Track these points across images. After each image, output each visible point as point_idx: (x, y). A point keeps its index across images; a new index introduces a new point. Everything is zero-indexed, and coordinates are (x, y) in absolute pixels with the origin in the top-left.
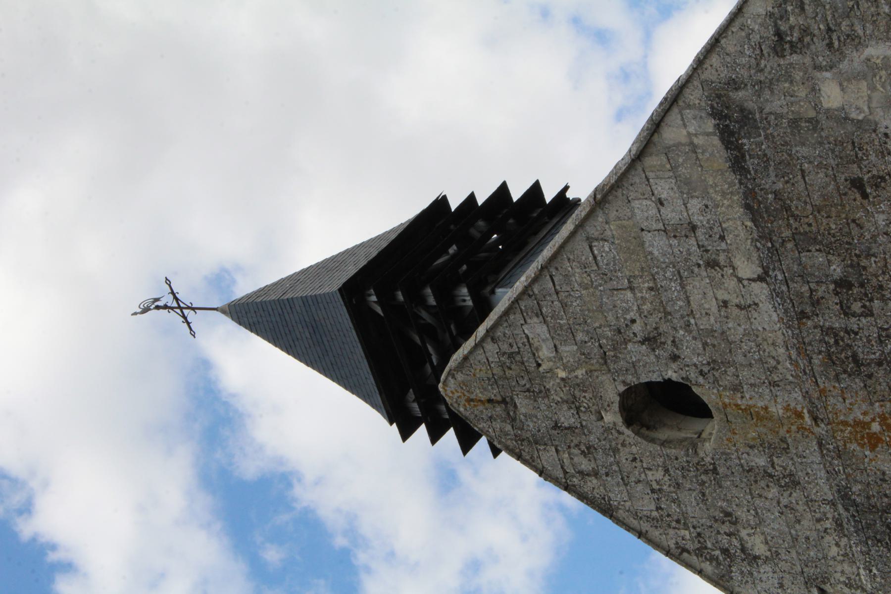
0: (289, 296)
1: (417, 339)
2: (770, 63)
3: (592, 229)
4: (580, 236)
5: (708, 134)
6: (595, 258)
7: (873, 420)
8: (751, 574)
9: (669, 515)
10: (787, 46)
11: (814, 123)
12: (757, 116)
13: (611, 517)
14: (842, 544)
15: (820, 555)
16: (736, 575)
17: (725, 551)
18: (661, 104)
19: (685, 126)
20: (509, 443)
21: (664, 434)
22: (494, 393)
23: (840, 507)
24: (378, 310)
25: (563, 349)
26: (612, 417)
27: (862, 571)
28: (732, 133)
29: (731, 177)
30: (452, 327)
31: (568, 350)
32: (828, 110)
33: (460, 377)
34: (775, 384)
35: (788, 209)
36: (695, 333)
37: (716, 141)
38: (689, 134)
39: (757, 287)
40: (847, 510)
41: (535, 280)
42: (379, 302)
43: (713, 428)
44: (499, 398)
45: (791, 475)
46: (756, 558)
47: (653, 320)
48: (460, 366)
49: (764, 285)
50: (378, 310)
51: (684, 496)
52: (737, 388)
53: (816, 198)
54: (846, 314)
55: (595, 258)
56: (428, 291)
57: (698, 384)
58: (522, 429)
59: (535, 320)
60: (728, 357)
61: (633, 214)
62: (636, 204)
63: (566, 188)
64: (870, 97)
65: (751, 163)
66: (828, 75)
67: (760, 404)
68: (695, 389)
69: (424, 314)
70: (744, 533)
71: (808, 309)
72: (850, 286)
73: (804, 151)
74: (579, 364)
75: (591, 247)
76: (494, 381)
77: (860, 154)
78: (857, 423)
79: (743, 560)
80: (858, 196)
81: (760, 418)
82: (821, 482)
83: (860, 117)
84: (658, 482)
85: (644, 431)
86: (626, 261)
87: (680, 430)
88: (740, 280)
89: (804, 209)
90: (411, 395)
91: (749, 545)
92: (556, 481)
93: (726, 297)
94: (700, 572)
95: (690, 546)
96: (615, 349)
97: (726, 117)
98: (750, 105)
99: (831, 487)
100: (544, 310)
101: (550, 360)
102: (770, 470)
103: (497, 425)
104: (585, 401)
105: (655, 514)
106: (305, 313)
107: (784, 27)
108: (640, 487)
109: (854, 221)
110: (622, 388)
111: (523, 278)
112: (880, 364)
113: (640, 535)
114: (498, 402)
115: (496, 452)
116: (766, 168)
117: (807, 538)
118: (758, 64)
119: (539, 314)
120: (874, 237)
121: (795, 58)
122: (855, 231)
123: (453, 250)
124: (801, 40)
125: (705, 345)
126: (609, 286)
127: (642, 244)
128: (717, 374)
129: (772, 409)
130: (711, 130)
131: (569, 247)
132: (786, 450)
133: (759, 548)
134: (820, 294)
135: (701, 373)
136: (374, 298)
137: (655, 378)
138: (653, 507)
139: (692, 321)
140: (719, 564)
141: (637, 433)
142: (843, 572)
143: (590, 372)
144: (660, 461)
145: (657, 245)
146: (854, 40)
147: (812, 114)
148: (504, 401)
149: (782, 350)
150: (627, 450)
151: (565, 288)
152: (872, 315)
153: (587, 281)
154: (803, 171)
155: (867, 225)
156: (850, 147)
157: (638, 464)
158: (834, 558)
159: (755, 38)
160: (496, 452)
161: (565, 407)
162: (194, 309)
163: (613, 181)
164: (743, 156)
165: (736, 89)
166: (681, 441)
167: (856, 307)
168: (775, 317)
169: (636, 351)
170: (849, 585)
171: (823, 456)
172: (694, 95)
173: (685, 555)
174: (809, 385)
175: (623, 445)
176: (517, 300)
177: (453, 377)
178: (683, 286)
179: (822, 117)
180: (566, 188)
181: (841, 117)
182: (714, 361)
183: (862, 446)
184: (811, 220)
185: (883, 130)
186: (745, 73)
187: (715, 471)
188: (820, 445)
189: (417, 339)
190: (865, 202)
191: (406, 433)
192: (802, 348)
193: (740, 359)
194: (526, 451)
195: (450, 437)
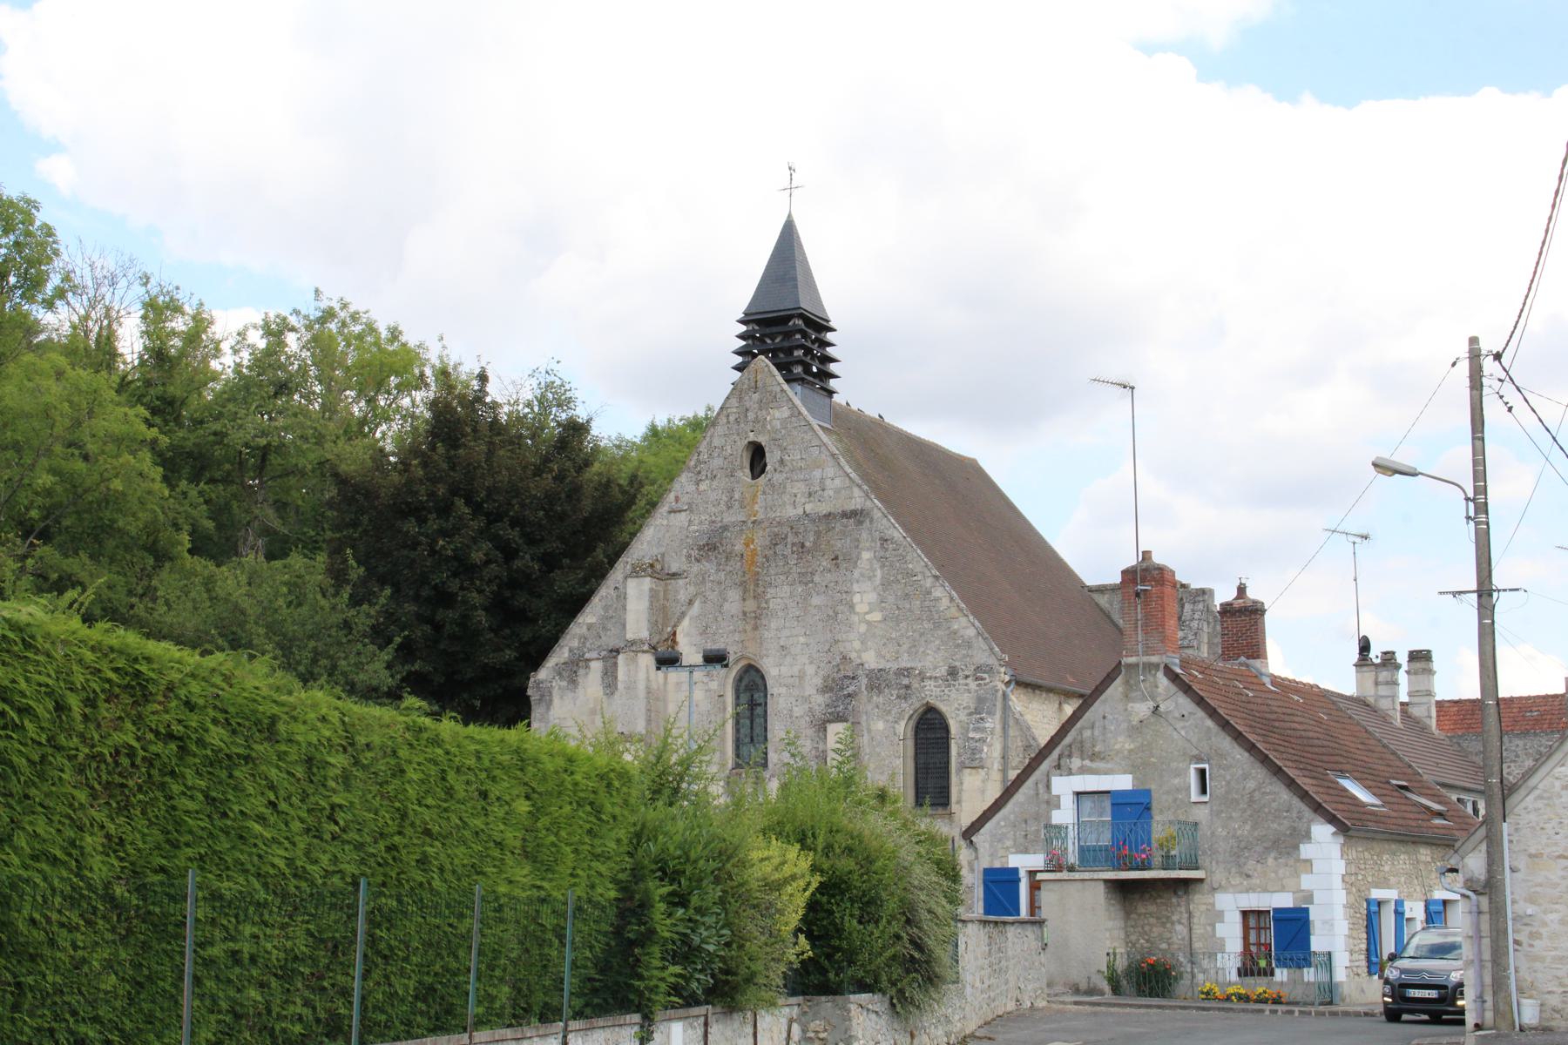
11: (857, 547)
17: (699, 472)
22: (760, 384)
26: (752, 437)
52: (764, 493)
76: (765, 385)
119: (792, 415)
133: (703, 487)
145: (817, 474)
146: (883, 566)
181: (858, 557)
195: (739, 359)
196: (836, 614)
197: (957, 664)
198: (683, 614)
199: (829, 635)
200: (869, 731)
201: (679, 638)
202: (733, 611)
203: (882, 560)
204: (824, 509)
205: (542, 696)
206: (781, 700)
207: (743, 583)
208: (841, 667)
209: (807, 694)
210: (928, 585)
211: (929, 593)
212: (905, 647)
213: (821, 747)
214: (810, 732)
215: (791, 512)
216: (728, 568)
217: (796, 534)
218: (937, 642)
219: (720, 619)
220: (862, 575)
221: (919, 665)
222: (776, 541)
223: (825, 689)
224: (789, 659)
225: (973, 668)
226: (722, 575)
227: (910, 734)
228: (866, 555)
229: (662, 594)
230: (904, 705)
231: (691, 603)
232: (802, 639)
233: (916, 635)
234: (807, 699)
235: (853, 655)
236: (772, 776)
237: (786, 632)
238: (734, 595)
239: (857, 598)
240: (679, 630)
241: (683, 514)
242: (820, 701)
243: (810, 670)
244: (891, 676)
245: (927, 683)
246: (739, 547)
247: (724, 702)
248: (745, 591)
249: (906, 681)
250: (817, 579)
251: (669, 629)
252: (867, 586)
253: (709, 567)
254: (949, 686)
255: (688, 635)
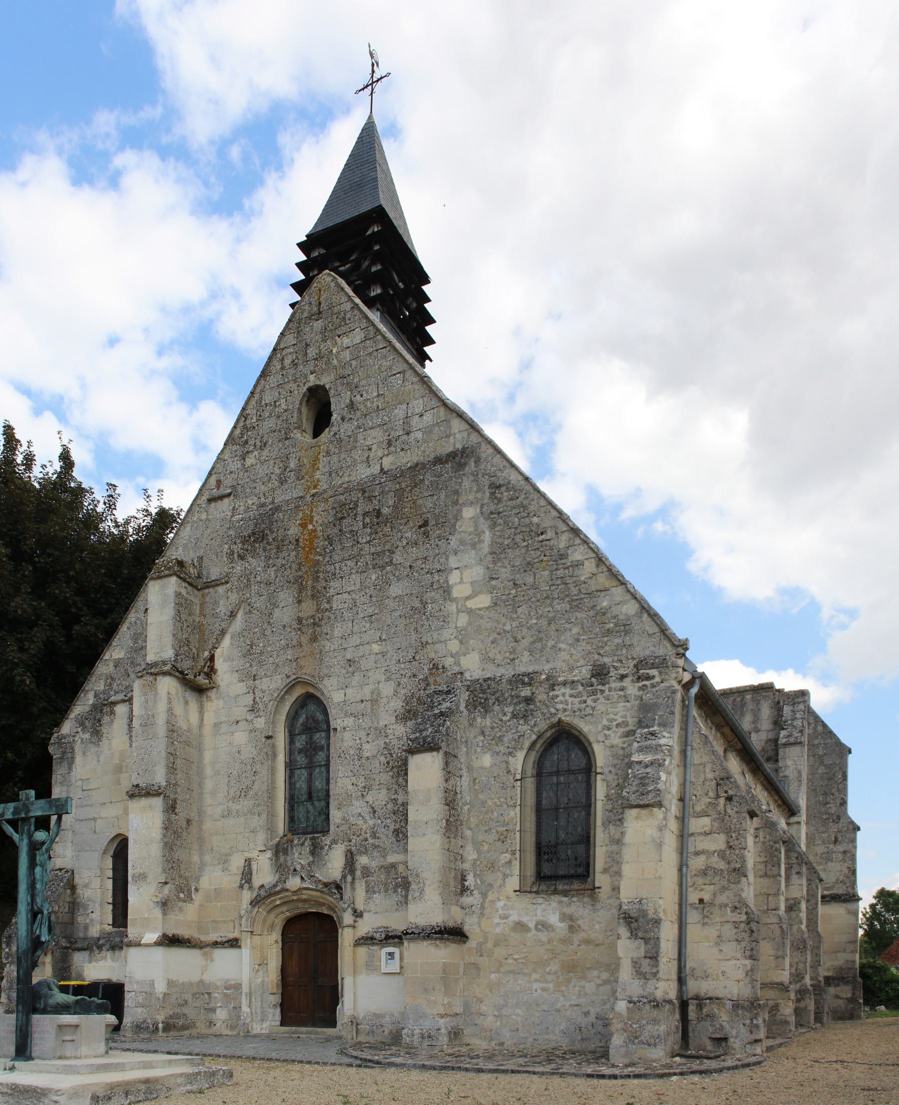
0: (378, 168)
1: (353, 258)
2: (486, 481)
3: (409, 373)
4: (406, 366)
5: (454, 445)
6: (395, 375)
7: (314, 526)
8: (236, 456)
9: (263, 411)
10: (493, 490)
11: (456, 503)
12: (461, 473)
13: (261, 376)
14: (253, 506)
15: (247, 494)
16: (235, 448)
17: (246, 442)
18: (471, 419)
19: (459, 432)
20: (298, 314)
21: (304, 410)
22: (324, 307)
23: (271, 506)
24: (369, 232)
25: (348, 351)
26: (312, 380)
27: (241, 516)
28: (454, 458)
29: (432, 456)
30: (359, 282)
31: (346, 355)
32: (461, 510)
33: (333, 285)
34: (330, 475)
35: (415, 486)
36: (355, 431)
37: (451, 449)
38: (455, 434)
39: (378, 467)
40: (270, 510)
41: (384, 337)
42: (373, 233)
43: (308, 439)
44: (321, 310)
45: (286, 481)
46: (244, 459)
47: (362, 407)
48: (338, 285)
49: (379, 472)
50: (369, 232)
51: (273, 420)
52: (328, 454)
53: (420, 502)
54: (364, 514)
55: (395, 375)
56: (379, 267)
57: (330, 431)
58: (305, 323)
59: (363, 336)
60: (343, 449)
61: (416, 399)
62: (421, 401)
63: (431, 360)
64: (466, 532)
65: (438, 467)
66: (478, 511)
67: (320, 466)
68: (327, 430)
69: (366, 263)
70: (256, 453)
71: (366, 495)
72: (378, 517)
73: (443, 497)
74: (340, 362)
75: (400, 373)
77: (440, 526)
78: (312, 517)
79: (242, 452)
80: (420, 523)
81: (314, 465)
82: (283, 497)
83: (457, 527)
84: (279, 405)
85: (306, 399)
86: (392, 393)
87: (307, 420)
88: (381, 458)
89: (415, 495)
90: (322, 251)
91: (250, 456)
92: (278, 343)
93: (373, 450)
94: (235, 427)
95: (248, 422)
96: (347, 384)
97: (462, 455)
98: (467, 469)
99: (281, 502)
100: (368, 342)
101: (342, 343)
102: (288, 470)
103: (307, 308)
104: (322, 364)
105: (263, 402)
106: (369, 179)
107: (503, 489)
108: (277, 394)
109: (408, 521)
110: (327, 387)
111: (385, 329)
112: (340, 531)
113: (252, 393)
114: (319, 309)
115: (292, 306)
116: (435, 476)
117: (255, 488)
118: (486, 474)
119: (366, 339)
120: (400, 531)
121: (488, 494)
122: (403, 521)
123: (401, 285)
124: (496, 498)
125: (349, 437)
126: (380, 382)
127: (400, 403)
128: (335, 442)
129: (318, 472)
130: (456, 447)
131: (400, 359)
132: (298, 479)
133: (250, 461)
134: (374, 501)
135: (336, 434)
136: (376, 229)
137: (333, 407)
138: (267, 402)
139: (361, 430)
140: (240, 438)
141: (304, 394)
142: (240, 506)
143: (335, 368)
144: (291, 407)
145: (400, 412)
146: (494, 525)
147: (460, 502)
148: (320, 313)
149: (347, 479)
150: (296, 388)
151: (379, 355)
152: (364, 528)
153: (383, 369)
154: (433, 495)
155: (406, 528)
156: (443, 521)
157: (289, 394)
158: (246, 502)
159: (499, 474)
160: (292, 306)
161: (317, 351)
162: (372, 94)
163: (433, 388)
164: (442, 464)
165: (475, 462)
166: (300, 420)
167: (367, 520)
168: (363, 476)
169: (346, 396)
170: (234, 509)
171: (296, 498)
172: (474, 438)
173: (243, 419)
174: (330, 493)
175: (298, 386)
176: (373, 325)
177: (333, 280)
178: (379, 426)
179: (458, 507)
180: (431, 360)
181: (457, 517)
182: (341, 441)
183: (301, 519)
184: (410, 498)
185: (450, 538)
186: (482, 467)
187: (287, 439)
188: (301, 497)
189: (353, 258)
190: (417, 527)
191: (301, 245)
192: (348, 490)
193: (343, 456)
194: (293, 325)
195: (300, 276)
196: (424, 604)
197: (607, 660)
198: (223, 633)
199: (414, 637)
200: (470, 769)
201: (219, 664)
202: (286, 620)
203: (493, 516)
204: (408, 459)
205: (64, 753)
206: (347, 735)
207: (299, 584)
208: (431, 680)
209: (382, 723)
210: (562, 546)
211: (563, 556)
212: (525, 643)
213: (401, 798)
214: (385, 778)
215: (363, 473)
216: (280, 562)
217: (370, 499)
218: (575, 630)
219: (268, 632)
220: (462, 542)
221: (547, 667)
222: (343, 512)
223: (407, 715)
224: (357, 677)
225: (632, 663)
226: (272, 571)
227: (530, 771)
228: (469, 513)
229: (197, 609)
230: (523, 728)
231: (233, 615)
232: (376, 648)
233: (544, 623)
234: (381, 732)
235: (448, 661)
236: (334, 842)
237: (355, 640)
238: (286, 597)
239: (454, 578)
240: (218, 653)
241: (226, 501)
242: (400, 732)
243: (387, 689)
244: (504, 686)
245: (559, 691)
246: (294, 530)
247: (274, 746)
248: (302, 588)
249: (526, 692)
250: (398, 558)
251: (206, 654)
252: (469, 557)
253: (255, 563)
254: (594, 693)
255: (229, 659)
